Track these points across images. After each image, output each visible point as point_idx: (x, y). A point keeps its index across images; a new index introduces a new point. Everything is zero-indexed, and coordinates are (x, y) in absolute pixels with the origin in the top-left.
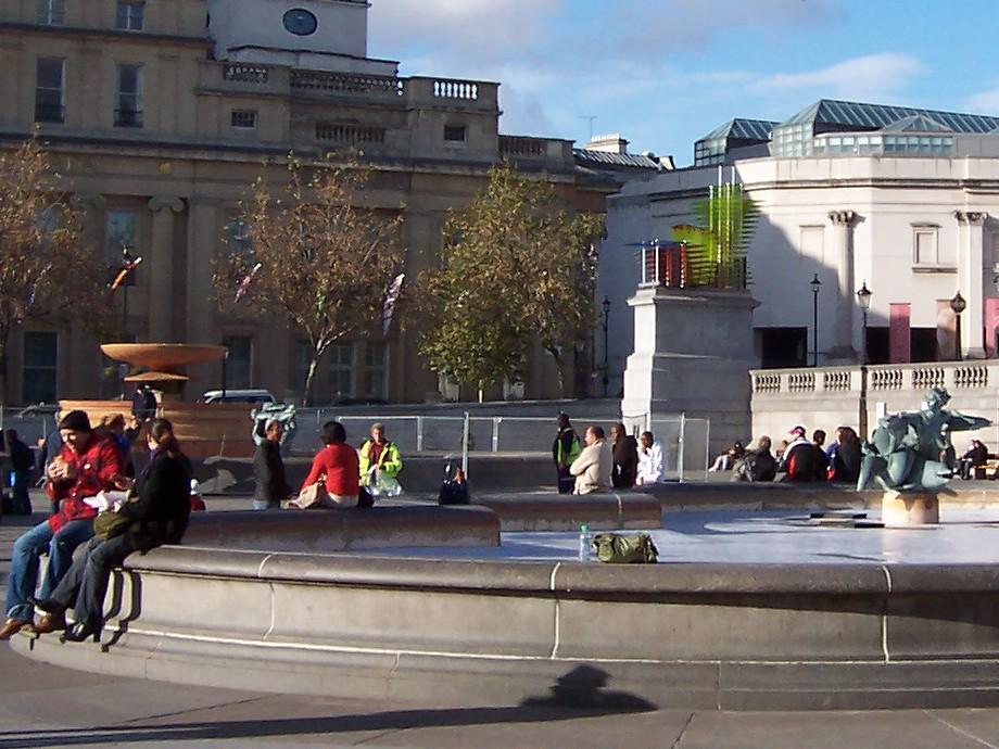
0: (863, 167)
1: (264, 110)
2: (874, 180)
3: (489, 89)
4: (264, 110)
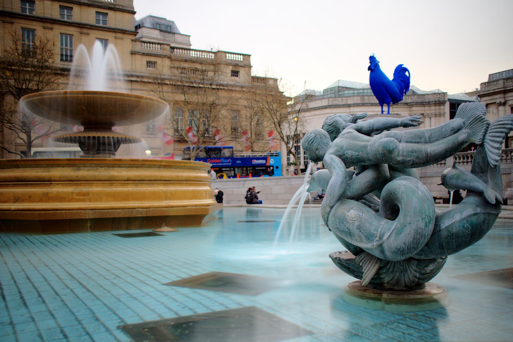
3: (247, 56)
4: (159, 60)
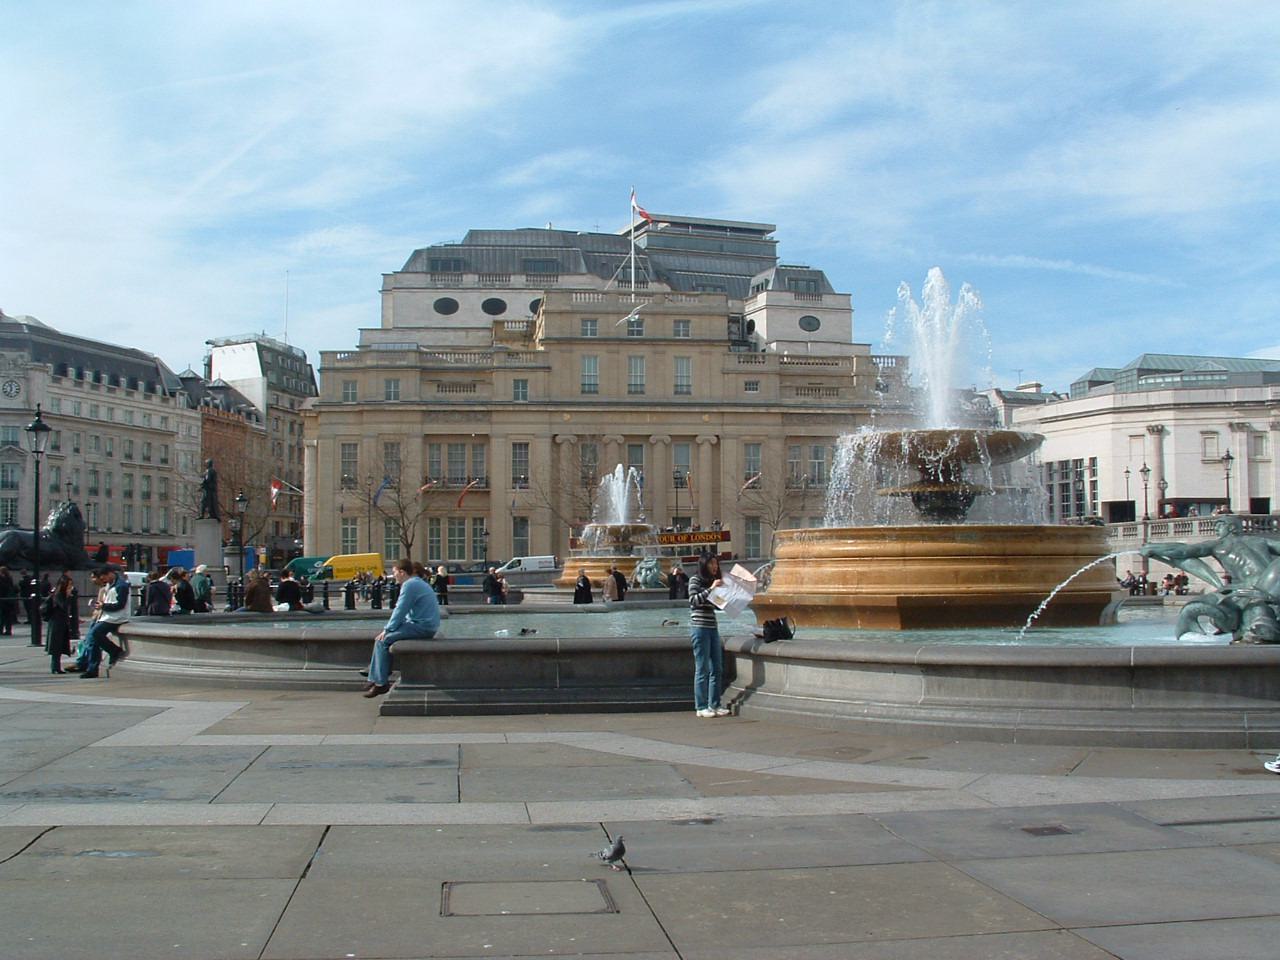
0: (1168, 397)
1: (763, 381)
2: (1175, 405)
